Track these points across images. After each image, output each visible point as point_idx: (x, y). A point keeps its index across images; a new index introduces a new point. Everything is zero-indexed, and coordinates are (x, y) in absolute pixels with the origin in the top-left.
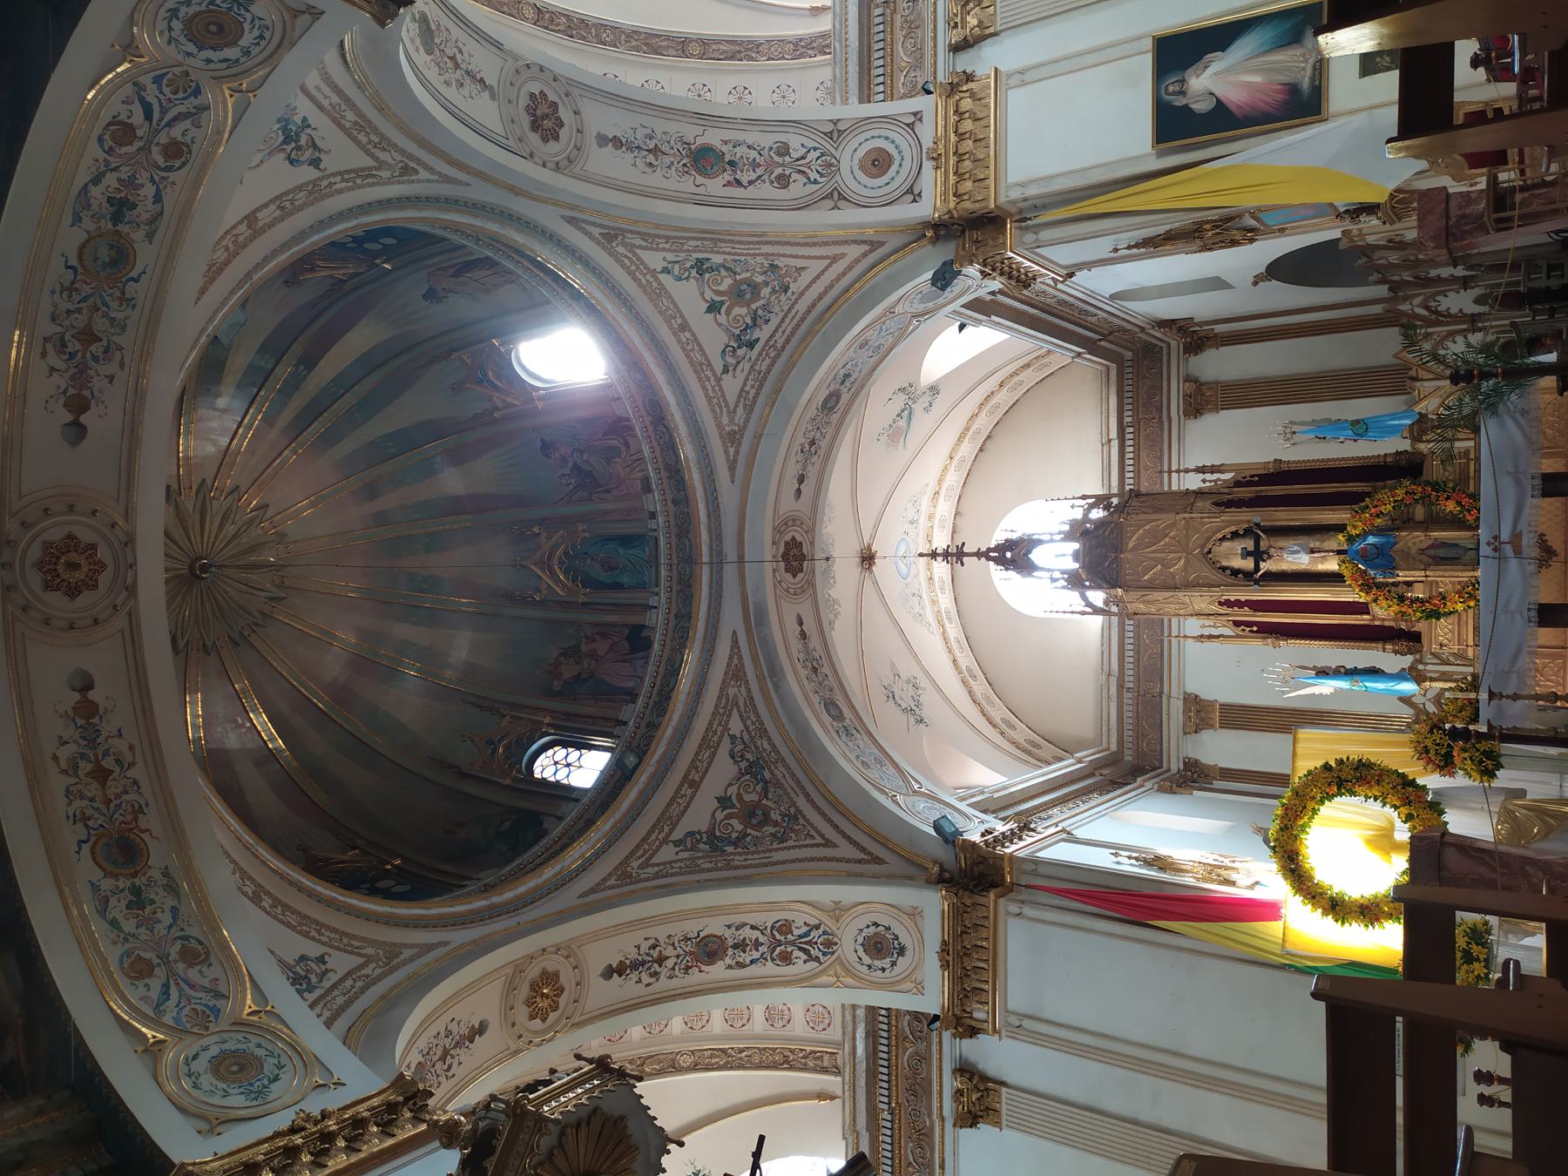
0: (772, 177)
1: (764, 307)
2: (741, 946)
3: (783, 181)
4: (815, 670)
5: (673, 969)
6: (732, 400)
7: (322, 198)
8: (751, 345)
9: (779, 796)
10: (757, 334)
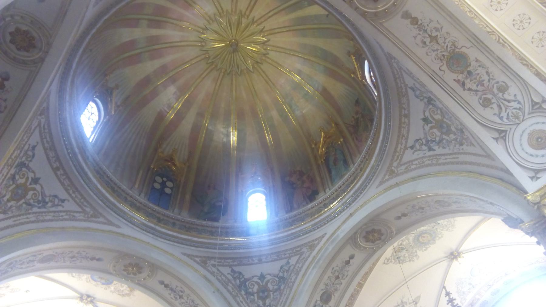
0: (483, 97)
1: (447, 141)
3: (486, 103)
5: (183, 303)
8: (430, 149)
9: (277, 298)
10: (436, 147)
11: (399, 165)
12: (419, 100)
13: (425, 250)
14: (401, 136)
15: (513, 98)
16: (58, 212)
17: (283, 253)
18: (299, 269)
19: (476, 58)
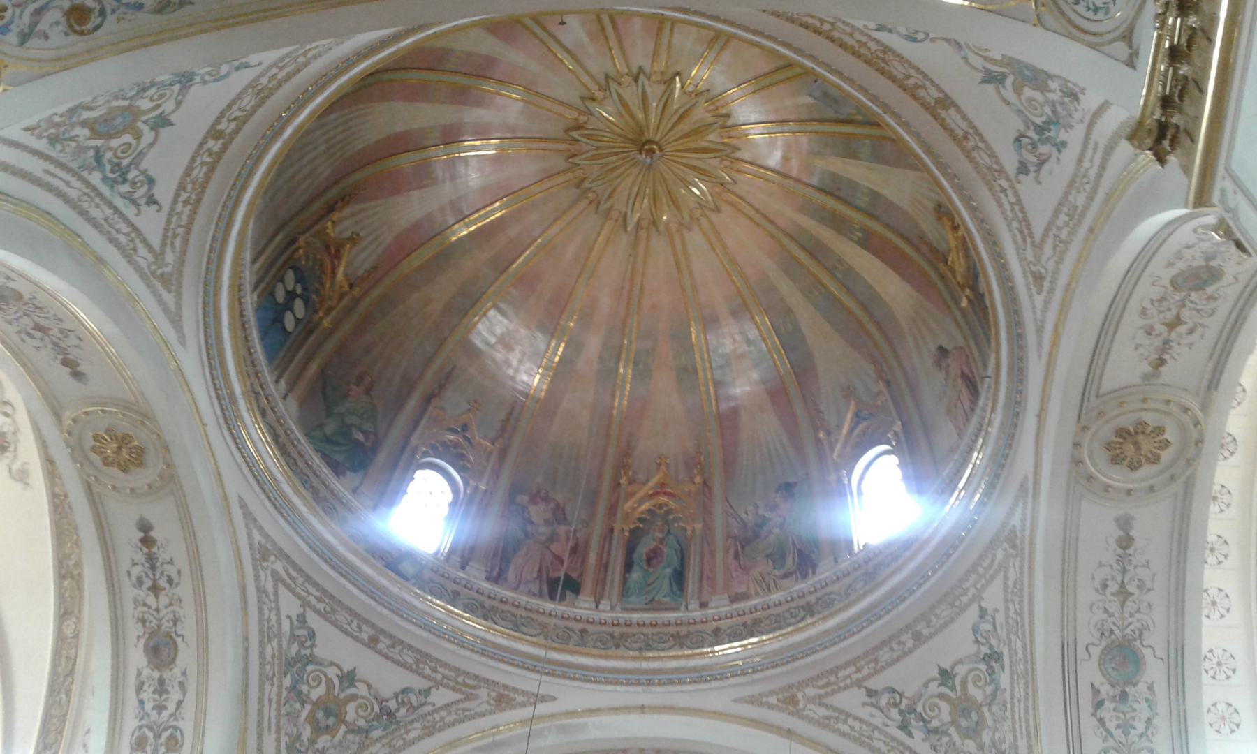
2: (161, 688)
5: (145, 604)
7: (988, 184)
8: (904, 727)
10: (918, 734)
14: (871, 657)
16: (122, 215)
17: (433, 665)
18: (441, 724)
19: (1153, 683)
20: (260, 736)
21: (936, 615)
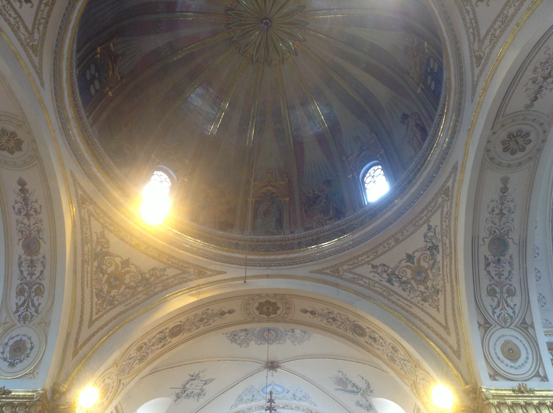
0: (493, 286)
2: (32, 264)
3: (492, 293)
4: (202, 320)
5: (22, 223)
6: (358, 270)
8: (389, 281)
10: (396, 284)
11: (349, 271)
12: (424, 240)
13: (259, 344)
14: (374, 251)
15: (512, 306)
19: (512, 255)
20: (83, 289)
21: (406, 230)
